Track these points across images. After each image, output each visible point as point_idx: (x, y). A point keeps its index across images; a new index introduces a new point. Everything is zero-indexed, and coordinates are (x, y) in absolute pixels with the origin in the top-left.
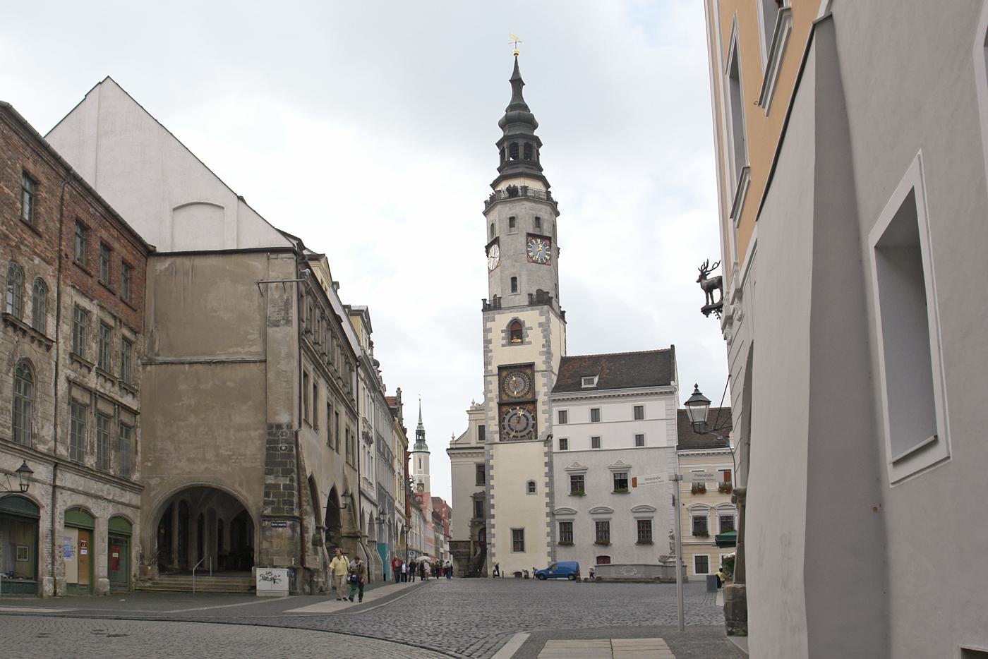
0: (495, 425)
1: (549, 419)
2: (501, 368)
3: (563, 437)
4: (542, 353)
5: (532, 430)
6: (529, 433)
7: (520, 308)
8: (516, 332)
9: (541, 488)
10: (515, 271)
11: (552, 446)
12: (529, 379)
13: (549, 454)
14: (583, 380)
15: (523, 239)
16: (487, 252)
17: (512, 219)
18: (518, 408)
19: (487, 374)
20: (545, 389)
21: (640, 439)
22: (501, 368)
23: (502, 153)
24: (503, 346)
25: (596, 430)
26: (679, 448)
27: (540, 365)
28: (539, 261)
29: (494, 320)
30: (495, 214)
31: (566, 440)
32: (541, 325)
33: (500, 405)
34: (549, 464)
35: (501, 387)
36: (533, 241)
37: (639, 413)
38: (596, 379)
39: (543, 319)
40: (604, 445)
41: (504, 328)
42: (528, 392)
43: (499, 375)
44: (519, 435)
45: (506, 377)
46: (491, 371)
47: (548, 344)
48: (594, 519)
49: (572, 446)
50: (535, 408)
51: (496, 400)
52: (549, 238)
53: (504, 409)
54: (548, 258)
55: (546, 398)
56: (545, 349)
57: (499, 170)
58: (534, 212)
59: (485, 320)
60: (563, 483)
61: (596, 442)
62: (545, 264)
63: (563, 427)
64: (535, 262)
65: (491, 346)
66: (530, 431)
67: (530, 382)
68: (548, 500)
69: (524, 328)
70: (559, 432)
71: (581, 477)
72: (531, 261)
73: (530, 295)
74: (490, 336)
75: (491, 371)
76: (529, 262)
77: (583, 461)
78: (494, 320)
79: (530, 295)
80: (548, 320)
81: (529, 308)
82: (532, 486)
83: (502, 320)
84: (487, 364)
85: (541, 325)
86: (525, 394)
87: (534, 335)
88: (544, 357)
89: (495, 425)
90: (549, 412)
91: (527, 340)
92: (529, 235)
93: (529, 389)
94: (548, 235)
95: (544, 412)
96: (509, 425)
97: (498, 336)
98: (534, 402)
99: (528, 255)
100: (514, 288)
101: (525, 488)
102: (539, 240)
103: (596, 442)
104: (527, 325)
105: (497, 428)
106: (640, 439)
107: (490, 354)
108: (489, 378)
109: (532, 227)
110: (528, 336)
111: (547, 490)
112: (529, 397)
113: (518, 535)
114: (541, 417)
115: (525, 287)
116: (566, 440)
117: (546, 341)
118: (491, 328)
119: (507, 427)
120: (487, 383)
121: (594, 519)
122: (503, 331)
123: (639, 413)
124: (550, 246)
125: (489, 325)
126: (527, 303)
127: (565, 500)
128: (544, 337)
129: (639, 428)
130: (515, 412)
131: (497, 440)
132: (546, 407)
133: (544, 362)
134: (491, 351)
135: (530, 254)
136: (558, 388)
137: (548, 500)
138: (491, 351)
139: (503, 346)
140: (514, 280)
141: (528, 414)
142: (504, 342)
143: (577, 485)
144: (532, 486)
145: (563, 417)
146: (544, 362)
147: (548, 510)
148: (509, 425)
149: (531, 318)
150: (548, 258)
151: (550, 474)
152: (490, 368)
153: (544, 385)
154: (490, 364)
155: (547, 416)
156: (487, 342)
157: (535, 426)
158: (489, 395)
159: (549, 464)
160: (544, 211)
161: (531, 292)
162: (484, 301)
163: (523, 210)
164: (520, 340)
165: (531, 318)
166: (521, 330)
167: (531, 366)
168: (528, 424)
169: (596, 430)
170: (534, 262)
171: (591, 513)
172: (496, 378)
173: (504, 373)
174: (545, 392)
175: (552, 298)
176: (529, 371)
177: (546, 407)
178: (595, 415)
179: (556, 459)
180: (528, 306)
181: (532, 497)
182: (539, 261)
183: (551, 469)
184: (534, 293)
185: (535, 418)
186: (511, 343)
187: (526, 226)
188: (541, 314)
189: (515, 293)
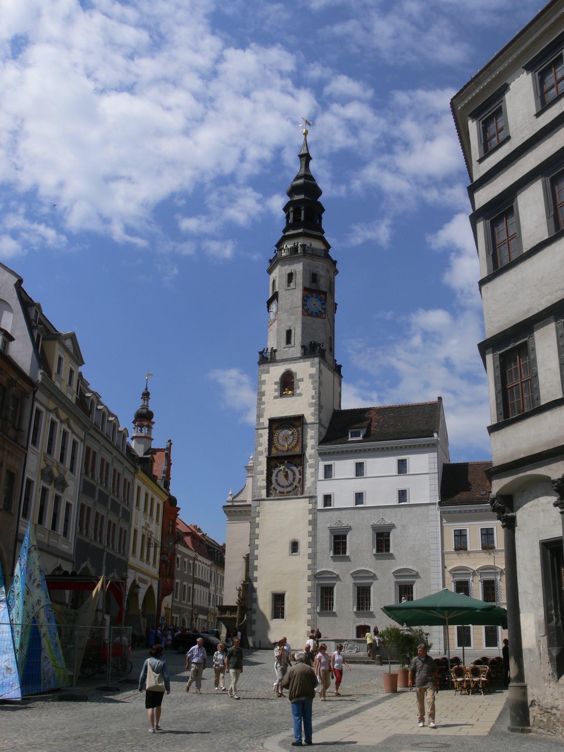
0: (263, 480)
2: (272, 421)
3: (327, 492)
4: (311, 405)
6: (296, 489)
9: (304, 548)
10: (290, 324)
11: (316, 503)
13: (314, 512)
15: (298, 294)
16: (268, 307)
17: (290, 277)
18: (286, 462)
21: (402, 495)
22: (272, 421)
23: (288, 217)
24: (275, 398)
25: (359, 485)
26: (440, 504)
27: (310, 418)
28: (314, 314)
29: (268, 372)
31: (330, 496)
33: (270, 459)
34: (313, 523)
36: (309, 295)
37: (402, 467)
40: (368, 502)
41: (278, 380)
43: (270, 427)
44: (285, 490)
46: (263, 423)
49: (336, 503)
51: (266, 454)
52: (325, 293)
54: (323, 311)
57: (285, 231)
61: (359, 497)
62: (320, 317)
63: (328, 482)
68: (310, 562)
69: (295, 380)
71: (345, 537)
75: (263, 423)
77: (346, 520)
78: (268, 372)
79: (303, 347)
81: (301, 360)
82: (295, 546)
85: (311, 376)
89: (263, 480)
91: (298, 391)
94: (324, 289)
96: (276, 480)
100: (288, 341)
101: (287, 548)
102: (314, 295)
103: (359, 497)
104: (299, 377)
105: (264, 484)
106: (402, 495)
107: (262, 406)
108: (260, 431)
110: (299, 388)
111: (310, 551)
112: (298, 450)
113: (278, 600)
114: (309, 471)
116: (330, 496)
122: (276, 383)
123: (402, 467)
124: (325, 300)
126: (299, 355)
129: (403, 482)
131: (264, 495)
134: (264, 403)
135: (305, 307)
137: (310, 562)
138: (264, 403)
139: (275, 398)
140: (289, 333)
143: (339, 543)
144: (295, 546)
145: (328, 471)
147: (310, 573)
148: (276, 480)
150: (323, 311)
152: (262, 420)
154: (262, 417)
155: (313, 470)
157: (302, 481)
160: (320, 267)
161: (304, 344)
166: (293, 382)
169: (359, 485)
170: (308, 315)
172: (267, 431)
173: (275, 426)
174: (312, 445)
175: (324, 351)
178: (360, 470)
179: (321, 517)
180: (300, 358)
181: (295, 558)
182: (314, 314)
183: (315, 528)
186: (282, 395)
188: (312, 365)
189: (289, 345)
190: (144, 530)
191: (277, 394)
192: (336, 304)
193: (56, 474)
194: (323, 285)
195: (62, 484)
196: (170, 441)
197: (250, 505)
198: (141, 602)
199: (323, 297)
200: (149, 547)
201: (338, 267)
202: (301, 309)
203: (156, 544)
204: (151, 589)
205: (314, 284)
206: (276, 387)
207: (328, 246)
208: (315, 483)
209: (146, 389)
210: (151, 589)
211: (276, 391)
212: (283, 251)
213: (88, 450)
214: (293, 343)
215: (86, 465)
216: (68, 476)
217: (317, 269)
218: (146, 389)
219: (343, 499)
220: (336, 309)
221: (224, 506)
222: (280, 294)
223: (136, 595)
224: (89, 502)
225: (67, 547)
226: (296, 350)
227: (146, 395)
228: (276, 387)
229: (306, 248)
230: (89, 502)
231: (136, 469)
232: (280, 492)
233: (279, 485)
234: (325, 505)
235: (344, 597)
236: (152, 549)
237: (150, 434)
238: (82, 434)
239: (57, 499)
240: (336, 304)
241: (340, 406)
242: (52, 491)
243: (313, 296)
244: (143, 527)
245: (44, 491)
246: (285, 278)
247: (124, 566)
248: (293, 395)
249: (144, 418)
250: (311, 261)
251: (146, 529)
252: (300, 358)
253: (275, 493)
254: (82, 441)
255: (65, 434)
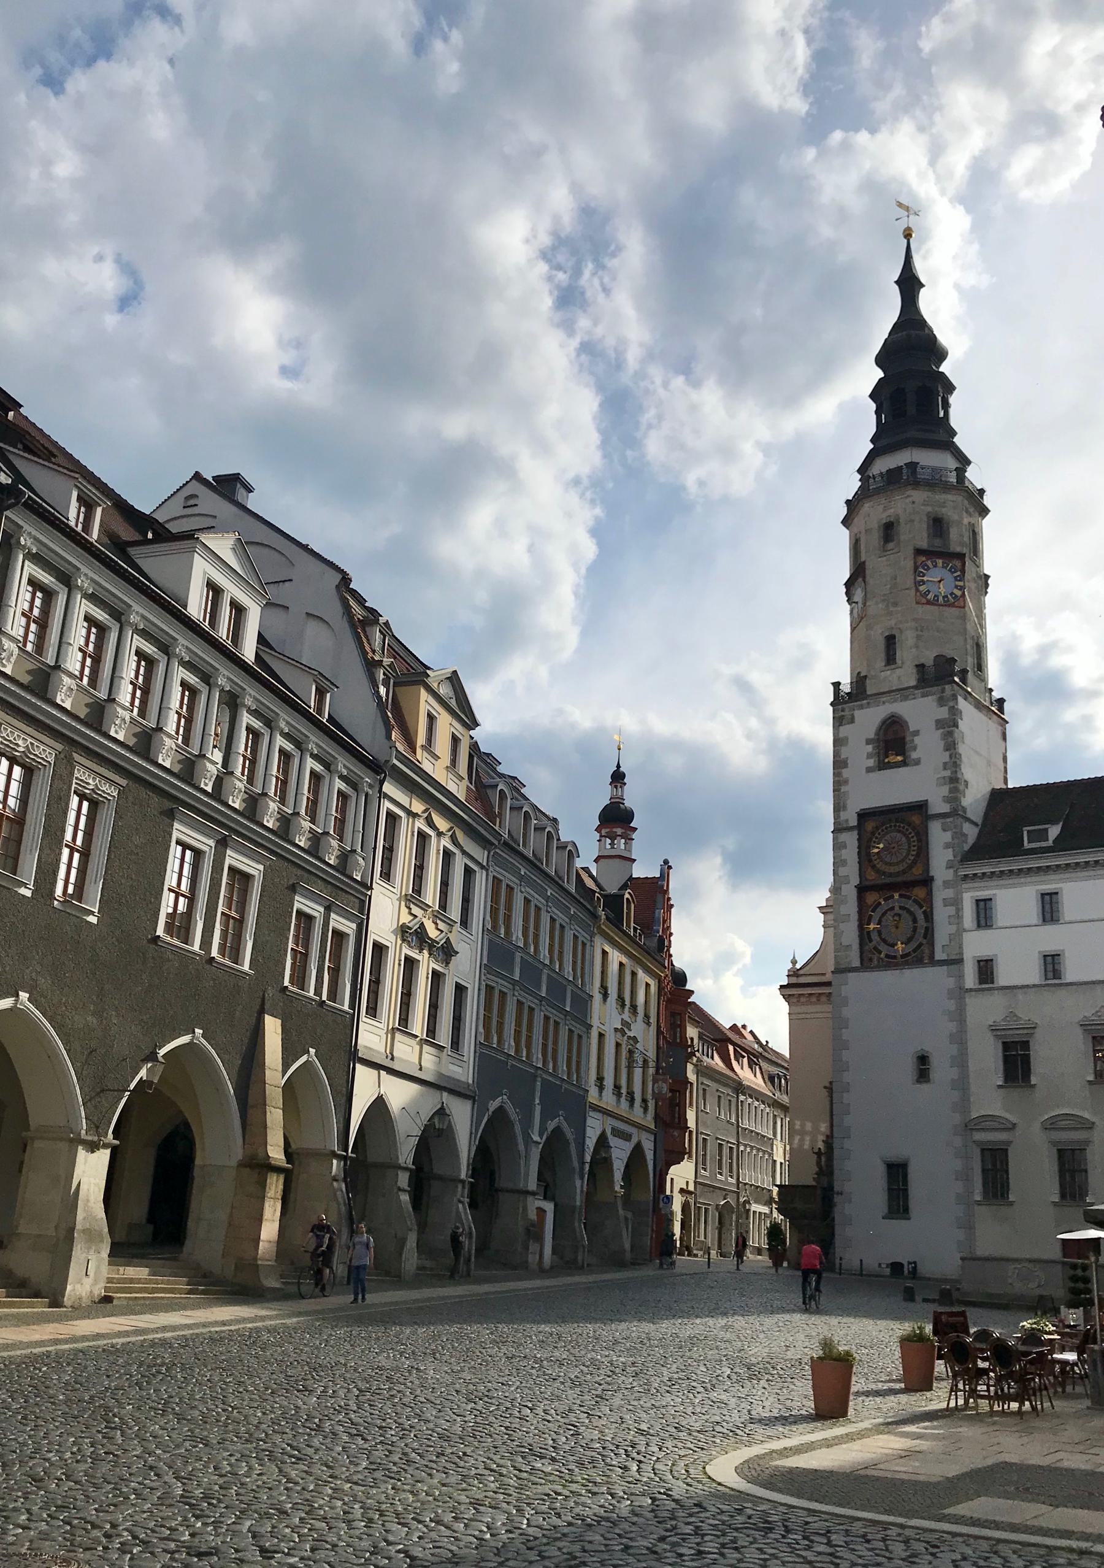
1: (958, 916)
3: (985, 952)
4: (943, 781)
5: (924, 942)
6: (920, 951)
7: (903, 693)
8: (893, 744)
9: (942, 1070)
11: (961, 977)
12: (918, 834)
13: (960, 993)
14: (1025, 833)
19: (838, 830)
20: (949, 855)
22: (864, 816)
24: (869, 770)
27: (938, 806)
28: (941, 599)
29: (852, 720)
30: (859, 521)
32: (940, 724)
33: (862, 890)
35: (863, 853)
36: (929, 563)
38: (1054, 831)
39: (943, 713)
41: (872, 735)
42: (914, 862)
43: (860, 827)
45: (873, 833)
46: (847, 821)
47: (954, 763)
48: (1054, 1143)
49: (1004, 976)
50: (930, 893)
51: (855, 880)
52: (961, 557)
53: (871, 898)
54: (958, 593)
55: (949, 875)
56: (948, 773)
58: (929, 509)
59: (839, 721)
60: (987, 1059)
62: (952, 605)
64: (934, 602)
65: (846, 773)
66: (921, 945)
67: (919, 840)
70: (977, 945)
71: (1025, 1045)
72: (924, 601)
73: (920, 667)
74: (845, 753)
75: (847, 821)
76: (917, 603)
77: (1030, 1010)
78: (852, 721)
79: (920, 667)
80: (955, 712)
83: (869, 719)
84: (838, 808)
85: (940, 724)
86: (910, 867)
87: (927, 745)
88: (945, 790)
90: (956, 903)
91: (914, 755)
92: (919, 552)
93: (918, 855)
95: (946, 903)
97: (861, 754)
98: (927, 882)
99: (917, 590)
100: (890, 659)
102: (940, 562)
109: (925, 535)
112: (917, 871)
114: (941, 914)
115: (908, 654)
117: (951, 756)
118: (847, 738)
119: (875, 937)
120: (837, 847)
121: (1054, 1143)
122: (868, 742)
124: (963, 571)
125: (845, 730)
127: (989, 1098)
128: (947, 749)
130: (890, 903)
132: (949, 893)
133: (947, 799)
135: (921, 588)
136: (977, 853)
138: (846, 782)
139: (869, 770)
140: (891, 641)
141: (914, 908)
142: (871, 763)
143: (1017, 1062)
146: (947, 799)
147: (957, 1119)
149: (920, 713)
150: (958, 593)
151: (960, 1038)
152: (843, 816)
153: (947, 846)
154: (845, 808)
155: (951, 910)
156: (839, 763)
157: (929, 933)
158: (842, 871)
159: (959, 1016)
161: (922, 661)
162: (836, 685)
163: (909, 506)
164: (900, 758)
165: (920, 713)
166: (904, 738)
167: (920, 807)
168: (915, 930)
170: (929, 603)
171: (1051, 1125)
173: (870, 826)
176: (916, 819)
177: (949, 893)
180: (916, 687)
182: (941, 599)
184: (929, 661)
185: (929, 916)
186: (882, 766)
187: (917, 535)
188: (941, 702)
189: (893, 666)
190: (619, 1035)
191: (871, 763)
192: (987, 577)
193: (432, 933)
194: (956, 540)
195: (446, 952)
196: (666, 862)
197: (828, 984)
198: (618, 1175)
199: (958, 564)
200: (630, 1068)
201: (987, 501)
202: (913, 592)
203: (645, 1061)
204: (638, 1149)
205: (937, 542)
206: (870, 748)
207: (964, 461)
208: (957, 937)
209: (618, 766)
210: (638, 1149)
211: (869, 756)
212: (871, 481)
213: (497, 882)
214: (899, 662)
215: (494, 912)
216: (457, 937)
217: (944, 510)
218: (618, 766)
219: (1018, 967)
220: (987, 585)
221: (782, 987)
222: (869, 566)
223: (607, 1162)
224: (500, 985)
225: (460, 1070)
226: (906, 676)
227: (618, 777)
228: (870, 748)
229: (919, 470)
230: (500, 985)
231: (595, 916)
232: (887, 956)
233: (884, 941)
234: (982, 981)
235: (1034, 1174)
236: (638, 1072)
237: (630, 851)
238: (481, 855)
239: (437, 978)
240: (987, 577)
241: (1006, 781)
242: (426, 964)
243: (935, 566)
244: (616, 1030)
245: (410, 964)
246: (876, 538)
247: (578, 1107)
248: (904, 763)
249: (616, 819)
250: (930, 493)
251: (623, 1033)
252: (916, 687)
253: (879, 959)
254: (482, 867)
255: (447, 855)
